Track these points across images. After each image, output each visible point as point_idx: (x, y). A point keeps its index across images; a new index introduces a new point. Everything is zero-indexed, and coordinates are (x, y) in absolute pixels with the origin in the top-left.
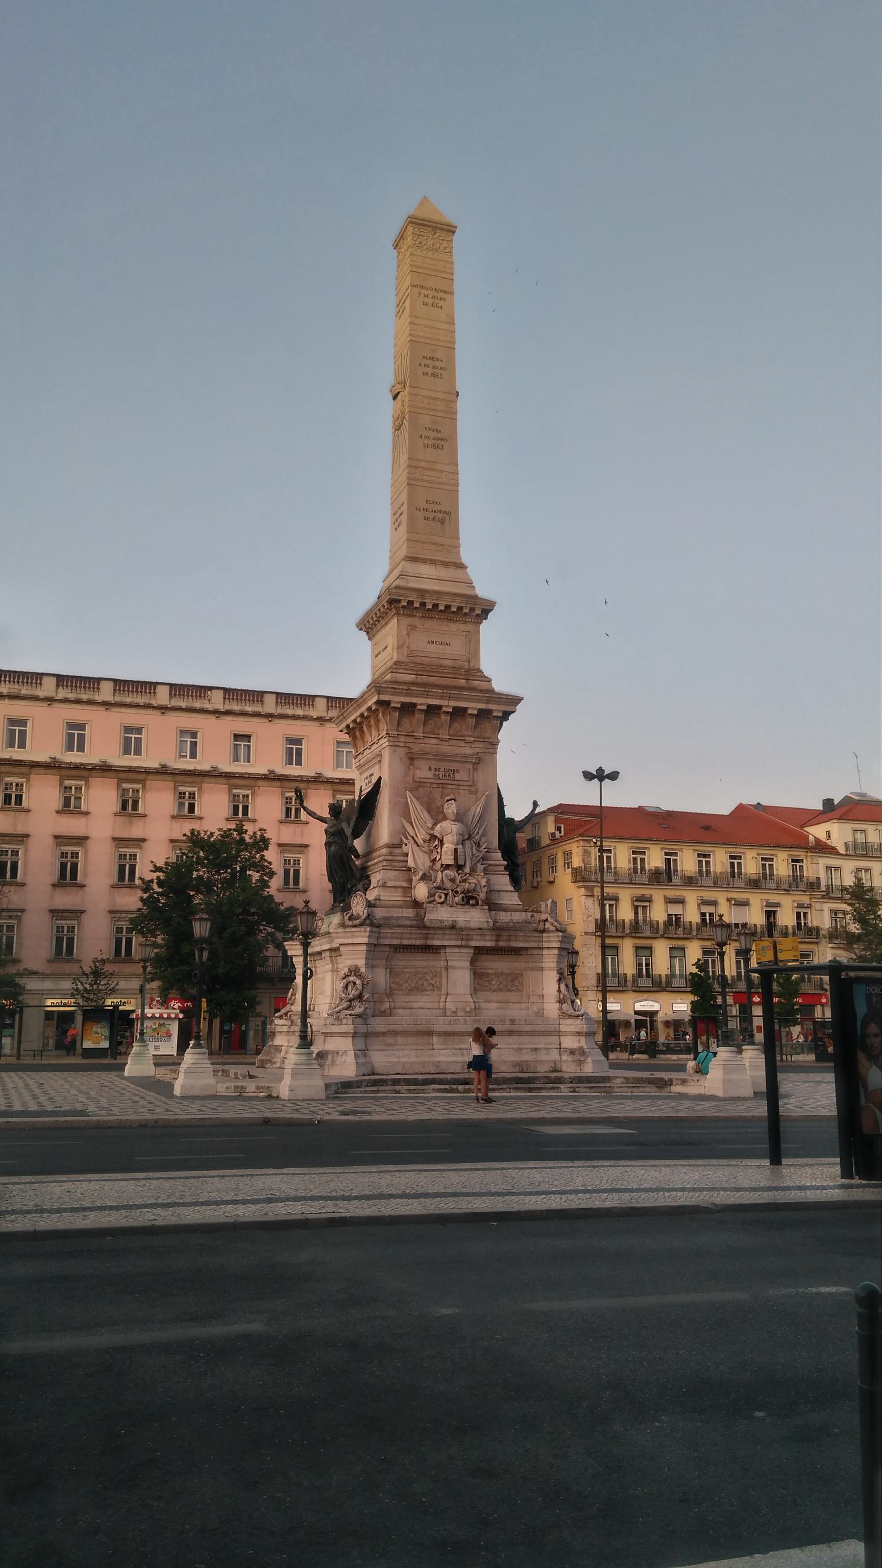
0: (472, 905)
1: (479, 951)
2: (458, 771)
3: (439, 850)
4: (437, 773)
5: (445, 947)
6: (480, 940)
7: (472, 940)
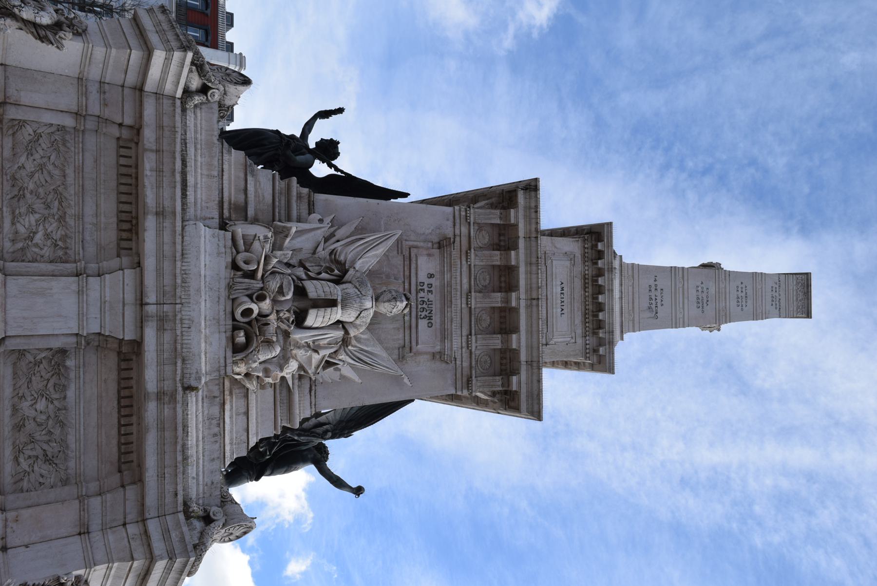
0: (233, 338)
1: (129, 354)
2: (430, 325)
3: (324, 275)
4: (426, 288)
5: (138, 265)
6: (160, 351)
7: (161, 329)
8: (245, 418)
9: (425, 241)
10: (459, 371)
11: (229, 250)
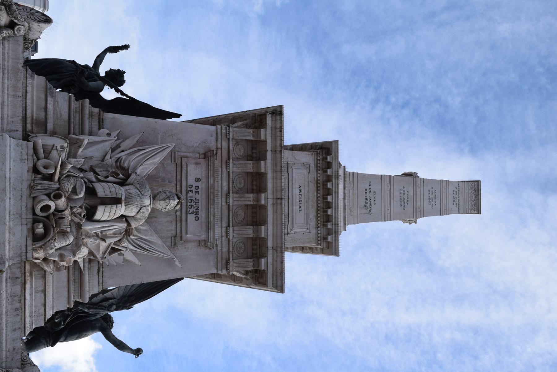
0: (33, 230)
2: (197, 219)
3: (110, 179)
4: (193, 189)
8: (43, 295)
9: (193, 152)
10: (220, 254)
11: (30, 157)
